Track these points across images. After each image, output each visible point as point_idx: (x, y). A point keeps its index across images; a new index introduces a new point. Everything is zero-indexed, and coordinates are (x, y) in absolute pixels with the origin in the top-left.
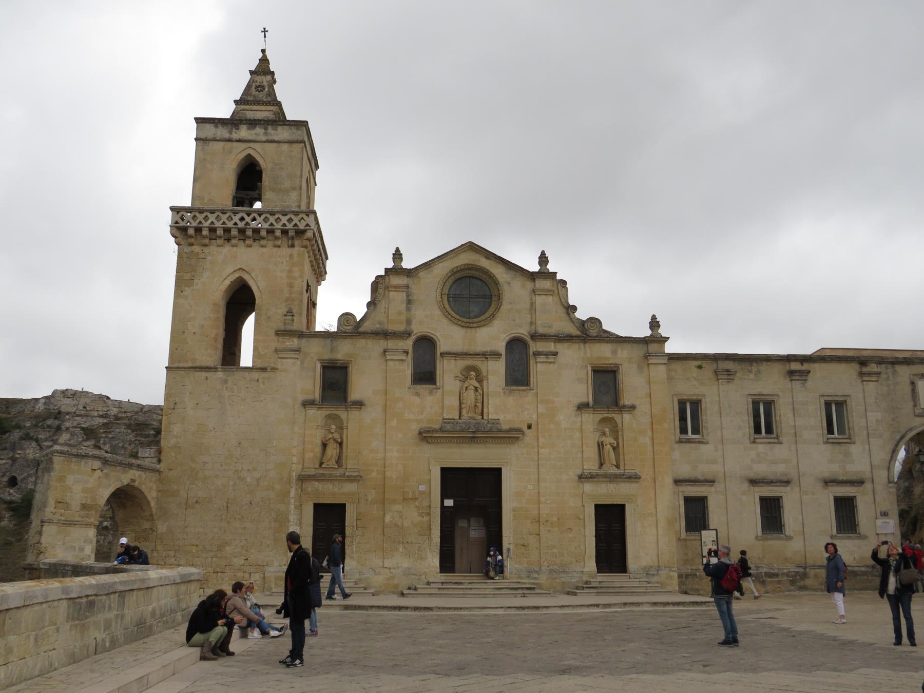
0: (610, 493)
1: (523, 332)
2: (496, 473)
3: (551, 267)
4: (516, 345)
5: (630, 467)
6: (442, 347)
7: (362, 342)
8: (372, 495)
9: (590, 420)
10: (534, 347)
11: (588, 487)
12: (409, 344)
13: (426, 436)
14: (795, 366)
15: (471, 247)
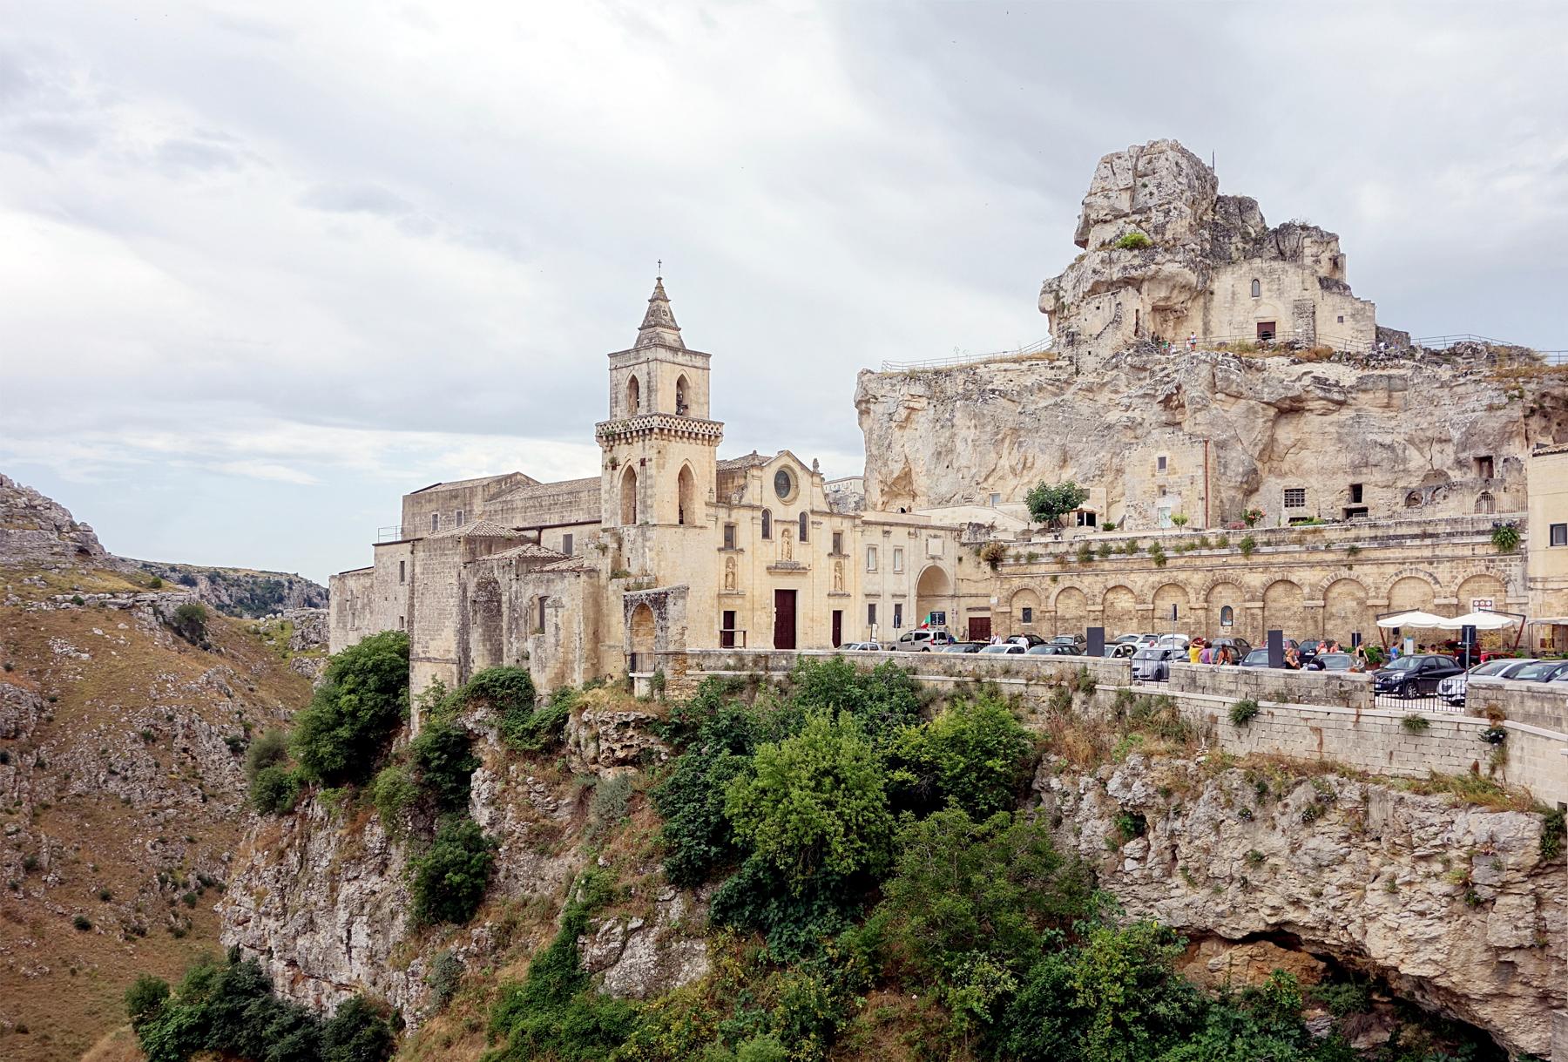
0: (837, 604)
1: (807, 509)
2: (793, 593)
3: (820, 470)
4: (803, 515)
5: (847, 590)
6: (774, 516)
7: (742, 511)
8: (748, 606)
9: (833, 561)
10: (811, 518)
11: (831, 601)
12: (759, 514)
13: (771, 570)
14: (887, 528)
15: (789, 454)
